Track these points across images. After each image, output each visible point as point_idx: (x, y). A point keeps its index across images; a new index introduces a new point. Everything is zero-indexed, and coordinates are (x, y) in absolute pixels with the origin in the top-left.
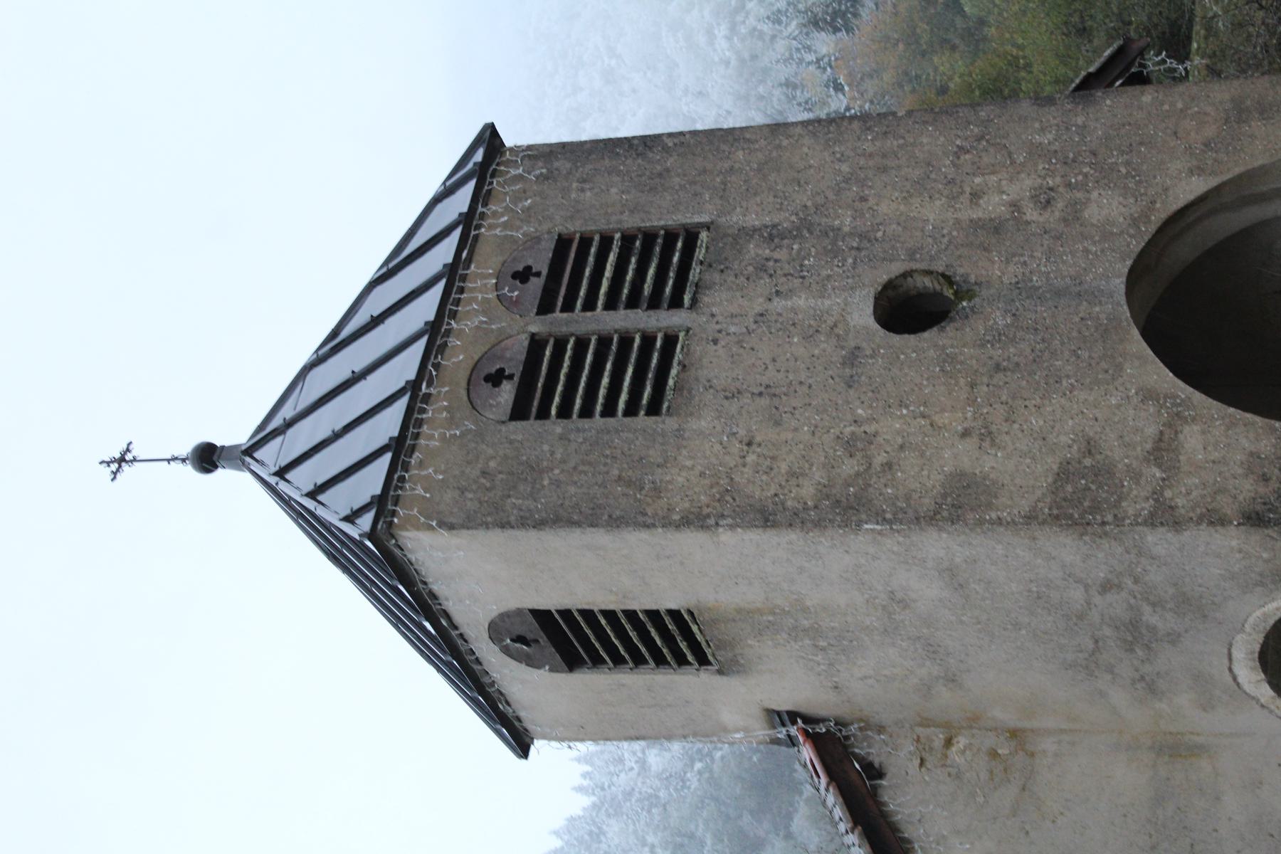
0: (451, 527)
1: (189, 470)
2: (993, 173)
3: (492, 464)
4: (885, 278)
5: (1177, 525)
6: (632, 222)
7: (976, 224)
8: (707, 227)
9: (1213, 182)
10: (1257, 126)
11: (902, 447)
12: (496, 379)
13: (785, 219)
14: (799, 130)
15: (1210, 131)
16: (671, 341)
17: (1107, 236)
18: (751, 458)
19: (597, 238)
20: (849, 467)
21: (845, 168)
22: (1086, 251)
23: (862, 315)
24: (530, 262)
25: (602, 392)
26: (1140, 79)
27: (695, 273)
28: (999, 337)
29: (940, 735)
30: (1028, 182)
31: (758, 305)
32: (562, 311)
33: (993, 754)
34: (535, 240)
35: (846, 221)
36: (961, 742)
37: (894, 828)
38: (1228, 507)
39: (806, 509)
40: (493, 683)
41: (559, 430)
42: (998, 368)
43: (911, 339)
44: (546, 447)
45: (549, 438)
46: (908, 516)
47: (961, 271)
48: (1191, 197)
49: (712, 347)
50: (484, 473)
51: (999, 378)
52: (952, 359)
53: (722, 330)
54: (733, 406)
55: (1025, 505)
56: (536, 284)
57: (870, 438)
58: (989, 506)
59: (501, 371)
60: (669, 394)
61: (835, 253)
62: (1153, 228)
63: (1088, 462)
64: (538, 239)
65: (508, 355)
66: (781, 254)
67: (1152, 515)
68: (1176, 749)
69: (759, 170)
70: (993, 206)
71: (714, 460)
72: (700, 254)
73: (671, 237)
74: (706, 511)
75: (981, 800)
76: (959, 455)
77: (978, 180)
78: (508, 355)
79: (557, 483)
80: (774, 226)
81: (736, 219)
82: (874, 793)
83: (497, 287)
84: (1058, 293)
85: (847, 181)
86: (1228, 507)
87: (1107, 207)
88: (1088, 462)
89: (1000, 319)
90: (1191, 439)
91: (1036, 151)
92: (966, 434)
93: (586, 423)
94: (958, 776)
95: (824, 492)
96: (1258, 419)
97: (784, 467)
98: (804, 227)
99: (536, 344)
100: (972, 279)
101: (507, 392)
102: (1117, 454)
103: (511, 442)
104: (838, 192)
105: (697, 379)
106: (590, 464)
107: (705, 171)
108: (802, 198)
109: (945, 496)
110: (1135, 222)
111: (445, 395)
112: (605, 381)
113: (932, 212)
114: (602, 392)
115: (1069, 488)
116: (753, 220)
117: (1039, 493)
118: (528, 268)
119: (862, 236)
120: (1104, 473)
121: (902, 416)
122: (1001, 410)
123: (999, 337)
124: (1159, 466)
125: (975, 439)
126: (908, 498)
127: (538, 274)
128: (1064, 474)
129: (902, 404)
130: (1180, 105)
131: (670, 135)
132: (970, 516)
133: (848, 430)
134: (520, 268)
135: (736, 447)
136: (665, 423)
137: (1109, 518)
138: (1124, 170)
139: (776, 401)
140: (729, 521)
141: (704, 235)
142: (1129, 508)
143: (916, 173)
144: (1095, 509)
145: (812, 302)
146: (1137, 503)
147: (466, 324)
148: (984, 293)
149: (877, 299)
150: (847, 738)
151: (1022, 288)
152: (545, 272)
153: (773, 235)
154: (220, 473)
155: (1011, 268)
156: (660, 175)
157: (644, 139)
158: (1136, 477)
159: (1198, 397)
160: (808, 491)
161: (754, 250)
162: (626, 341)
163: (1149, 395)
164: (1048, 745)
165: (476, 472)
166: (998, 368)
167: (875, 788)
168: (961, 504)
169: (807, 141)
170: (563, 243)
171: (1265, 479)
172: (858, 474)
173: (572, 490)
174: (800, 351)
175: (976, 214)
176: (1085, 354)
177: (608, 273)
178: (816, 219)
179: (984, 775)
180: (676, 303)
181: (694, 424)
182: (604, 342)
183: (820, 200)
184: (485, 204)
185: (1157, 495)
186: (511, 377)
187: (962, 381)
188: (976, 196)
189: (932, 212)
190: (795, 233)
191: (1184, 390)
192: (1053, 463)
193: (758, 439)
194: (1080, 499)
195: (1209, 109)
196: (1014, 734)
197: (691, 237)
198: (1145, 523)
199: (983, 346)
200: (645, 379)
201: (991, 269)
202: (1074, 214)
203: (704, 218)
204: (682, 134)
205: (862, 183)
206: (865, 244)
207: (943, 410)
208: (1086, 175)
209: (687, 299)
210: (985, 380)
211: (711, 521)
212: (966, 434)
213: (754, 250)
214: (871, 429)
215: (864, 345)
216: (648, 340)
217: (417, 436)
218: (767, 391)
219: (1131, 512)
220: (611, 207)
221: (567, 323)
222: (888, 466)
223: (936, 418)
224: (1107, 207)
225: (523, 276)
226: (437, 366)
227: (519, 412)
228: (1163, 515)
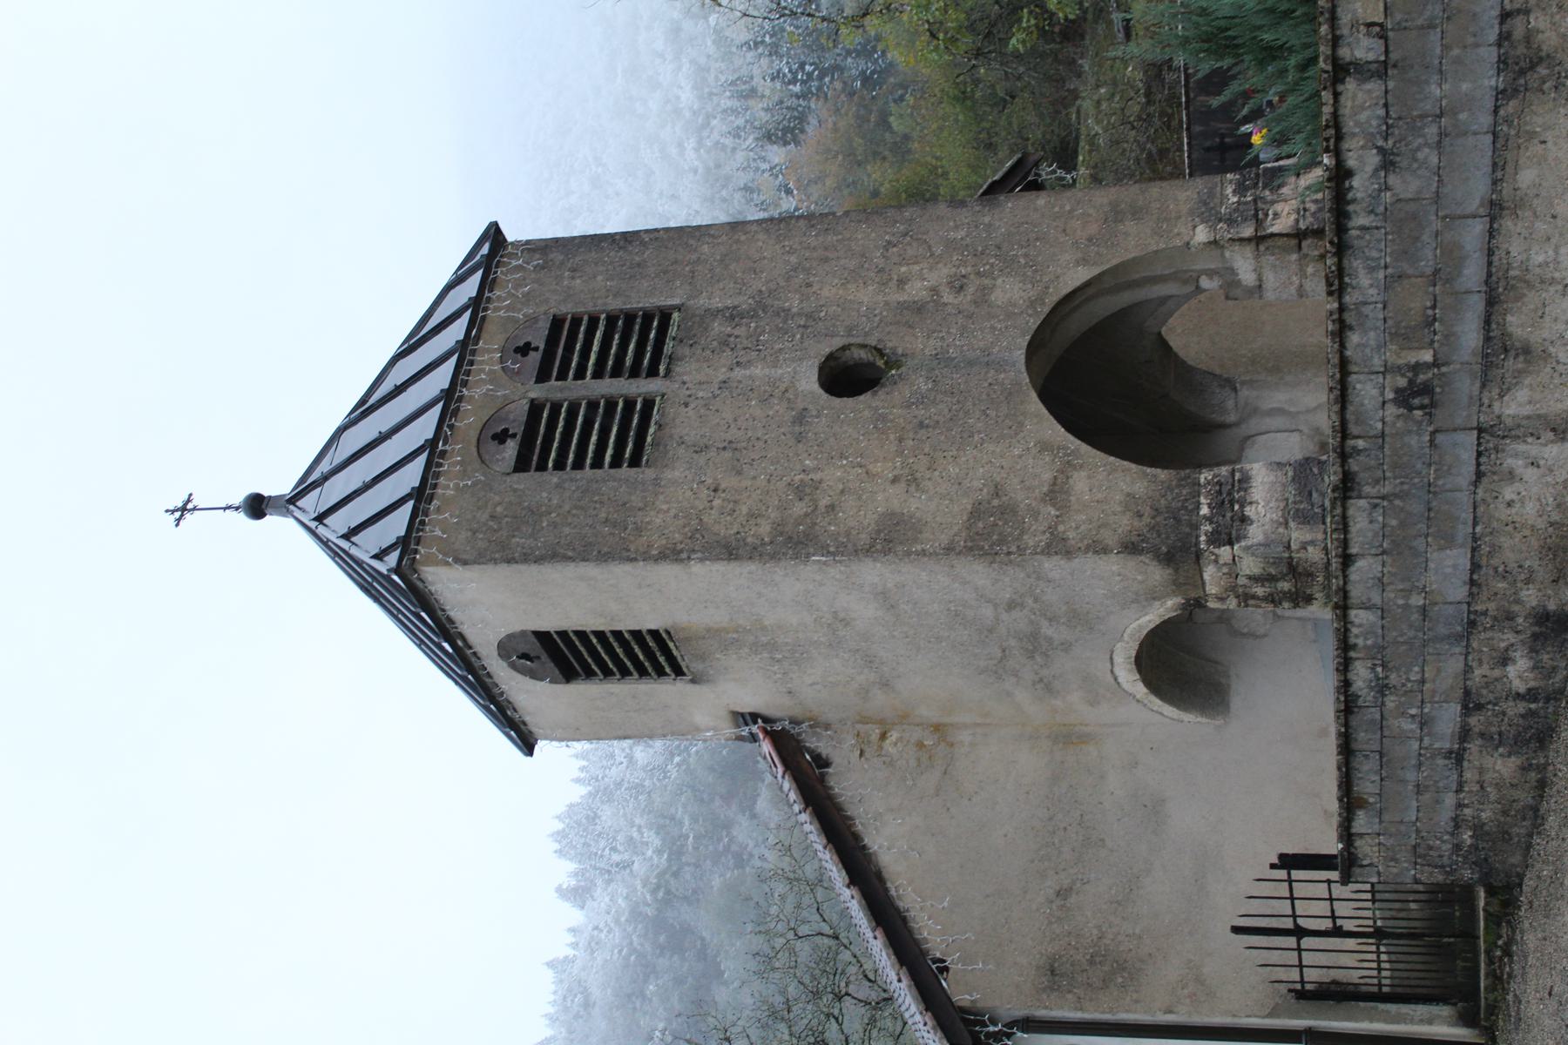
0: (465, 563)
1: (241, 518)
2: (916, 263)
3: (499, 509)
4: (828, 350)
5: (1068, 554)
6: (615, 304)
7: (902, 306)
8: (679, 308)
9: (1096, 271)
10: (1130, 226)
11: (842, 492)
12: (502, 437)
13: (745, 302)
14: (754, 228)
15: (1093, 229)
16: (649, 404)
17: (1009, 315)
18: (717, 502)
19: (586, 318)
20: (799, 509)
21: (793, 259)
22: (993, 328)
23: (809, 381)
24: (529, 339)
25: (591, 448)
26: (1036, 186)
27: (668, 347)
28: (921, 400)
29: (876, 730)
30: (945, 271)
31: (722, 374)
32: (557, 379)
33: (920, 745)
34: (532, 320)
35: (794, 303)
36: (894, 736)
37: (839, 808)
38: (1110, 538)
39: (763, 544)
40: (502, 694)
41: (555, 480)
42: (921, 425)
44: (544, 495)
45: (547, 489)
46: (847, 549)
47: (890, 345)
48: (1078, 283)
49: (683, 409)
50: (492, 517)
51: (923, 433)
52: (883, 418)
53: (694, 396)
54: (701, 459)
55: (944, 539)
56: (535, 358)
57: (816, 485)
58: (916, 540)
59: (506, 430)
60: (648, 449)
62: (1047, 310)
63: (996, 502)
64: (536, 319)
65: (511, 417)
67: (1048, 545)
68: (1069, 737)
69: (722, 261)
70: (916, 290)
71: (685, 504)
72: (673, 331)
73: (648, 317)
74: (679, 547)
75: (909, 783)
76: (889, 498)
77: (903, 269)
78: (511, 417)
79: (555, 525)
80: (735, 307)
81: (702, 302)
82: (822, 779)
83: (502, 360)
84: (971, 363)
85: (795, 270)
86: (1110, 538)
88: (996, 502)
89: (923, 385)
90: (1080, 483)
91: (951, 245)
92: (895, 480)
93: (578, 474)
94: (891, 764)
95: (778, 528)
96: (1133, 466)
97: (744, 510)
98: (761, 306)
99: (535, 408)
100: (900, 351)
101: (511, 449)
102: (1020, 496)
103: (515, 491)
104: (788, 279)
105: (671, 436)
106: (582, 508)
107: (676, 262)
108: (758, 284)
109: (879, 532)
110: (1032, 304)
111: (458, 451)
112: (594, 438)
113: (866, 295)
114: (591, 448)
115: (980, 525)
116: (717, 303)
117: (956, 529)
118: (528, 344)
119: (809, 316)
120: (1008, 511)
121: (843, 466)
122: (925, 460)
123: (921, 400)
124: (1054, 505)
125: (903, 485)
126: (848, 534)
127: (536, 349)
128: (976, 513)
129: (842, 456)
130: (1068, 208)
131: (647, 231)
132: (899, 548)
133: (798, 478)
134: (521, 344)
136: (646, 473)
137: (1014, 549)
138: (1022, 261)
139: (737, 454)
140: (699, 555)
141: (676, 315)
142: (1029, 540)
143: (852, 264)
144: (1002, 541)
145: (767, 371)
146: (1036, 537)
147: (476, 393)
149: (821, 369)
150: (799, 734)
151: (941, 358)
152: (542, 346)
153: (733, 315)
154: (270, 520)
155: (932, 342)
156: (639, 265)
157: (624, 234)
158: (1035, 514)
159: (1085, 448)
160: (765, 529)
161: (718, 327)
163: (1044, 447)
164: (965, 736)
165: (486, 516)
166: (921, 425)
167: (823, 775)
168: (891, 538)
169: (761, 236)
170: (557, 323)
171: (1140, 515)
172: (806, 515)
173: (567, 530)
174: (758, 412)
176: (992, 413)
177: (595, 348)
178: (769, 301)
179: (913, 763)
180: (653, 372)
181: (668, 474)
182: (593, 405)
183: (772, 286)
184: (491, 291)
185: (1052, 529)
186: (514, 436)
187: (892, 437)
188: (902, 282)
189: (866, 295)
191: (1073, 442)
192: (967, 503)
193: (723, 486)
194: (990, 533)
195: (1091, 211)
196: (938, 728)
198: (1042, 553)
199: (909, 407)
200: (628, 437)
201: (916, 343)
202: (982, 298)
203: (676, 301)
204: (656, 230)
205: (807, 271)
206: (811, 323)
207: (876, 461)
208: (992, 265)
209: (662, 368)
210: (911, 435)
211: (684, 555)
212: (895, 480)
213: (718, 327)
214: (817, 477)
215: (810, 407)
216: (630, 404)
217: (435, 486)
219: (1031, 543)
220: (598, 293)
221: (561, 390)
222: (831, 508)
223: (870, 467)
224: (1009, 291)
225: (524, 350)
226: (451, 427)
227: (522, 465)
228: (1057, 546)
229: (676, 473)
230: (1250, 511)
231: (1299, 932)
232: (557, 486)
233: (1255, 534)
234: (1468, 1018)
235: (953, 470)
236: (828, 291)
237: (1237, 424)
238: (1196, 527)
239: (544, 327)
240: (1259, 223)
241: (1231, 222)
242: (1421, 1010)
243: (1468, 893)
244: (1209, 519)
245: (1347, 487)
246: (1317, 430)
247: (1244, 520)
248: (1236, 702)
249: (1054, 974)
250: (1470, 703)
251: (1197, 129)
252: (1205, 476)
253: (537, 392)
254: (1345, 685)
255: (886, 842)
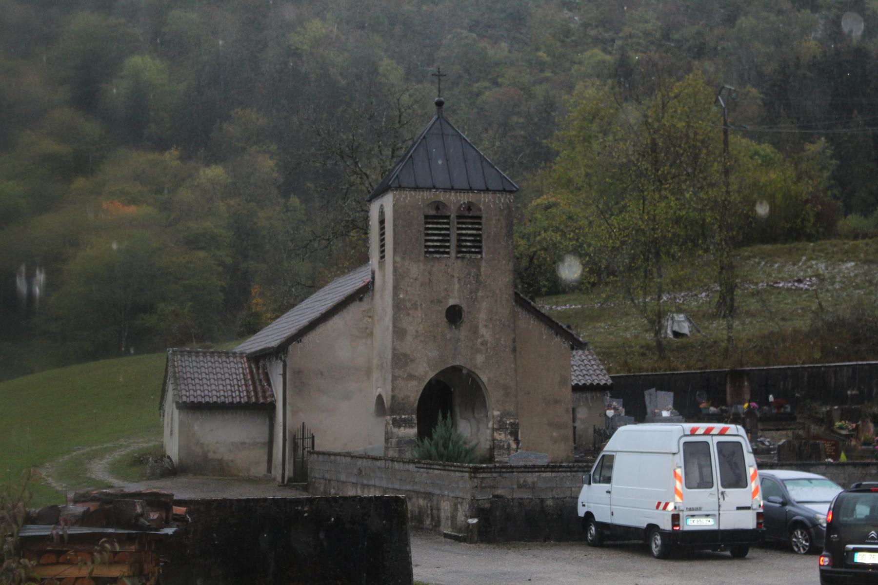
5: (392, 381)
6: (484, 237)
12: (437, 208)
13: (482, 278)
16: (448, 253)
20: (408, 305)
21: (498, 291)
23: (451, 302)
27: (468, 255)
29: (369, 314)
31: (456, 275)
33: (367, 328)
34: (480, 210)
35: (480, 294)
36: (370, 320)
43: (444, 315)
46: (396, 320)
53: (453, 265)
54: (426, 274)
55: (398, 347)
56: (466, 213)
61: (471, 293)
66: (472, 278)
68: (369, 372)
70: (483, 331)
72: (473, 256)
73: (480, 247)
76: (411, 330)
81: (483, 264)
87: (480, 359)
89: (448, 337)
92: (417, 331)
96: (418, 397)
98: (478, 282)
99: (448, 217)
101: (433, 212)
112: (436, 238)
113: (483, 316)
116: (482, 269)
128: (405, 355)
135: (415, 276)
136: (422, 258)
141: (479, 256)
142: (396, 370)
146: (397, 372)
148: (457, 332)
151: (458, 340)
153: (478, 275)
159: (425, 384)
162: (448, 241)
168: (399, 333)
175: (480, 327)
180: (459, 252)
185: (400, 376)
188: (486, 326)
189: (483, 316)
190: (478, 282)
191: (427, 380)
194: (400, 360)
196: (372, 333)
197: (480, 253)
200: (435, 250)
201: (464, 332)
202: (478, 351)
209: (459, 255)
212: (417, 331)
216: (448, 247)
218: (430, 281)
222: (408, 314)
225: (469, 209)
227: (426, 217)
228: (394, 378)
229: (422, 266)
230: (402, 428)
231: (303, 439)
232: (419, 231)
233: (395, 430)
234: (290, 480)
235: (420, 348)
236: (484, 305)
237: (474, 417)
238: (399, 414)
239: (478, 214)
240: (497, 430)
241: (499, 421)
242: (292, 468)
243: (306, 480)
244: (401, 418)
245: (352, 457)
246: (471, 441)
247: (399, 427)
248: (380, 419)
249: (298, 373)
250: (330, 480)
251: (789, 372)
252: (414, 416)
253: (453, 216)
254: (339, 454)
255: (336, 322)
